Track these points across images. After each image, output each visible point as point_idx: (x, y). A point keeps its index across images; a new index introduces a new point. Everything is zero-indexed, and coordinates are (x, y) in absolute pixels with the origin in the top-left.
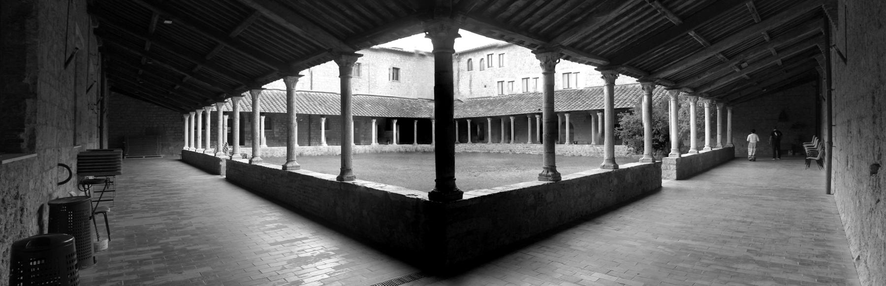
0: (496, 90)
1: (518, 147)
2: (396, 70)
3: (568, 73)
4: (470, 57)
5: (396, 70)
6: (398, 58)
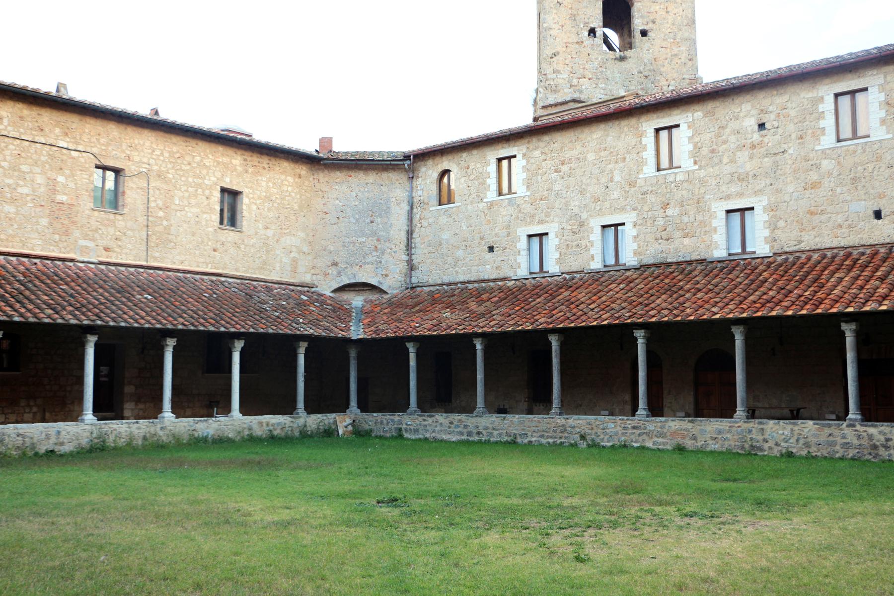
0: (522, 259)
1: (610, 427)
2: (231, 195)
3: (742, 211)
4: (445, 163)
5: (231, 195)
6: (237, 159)
